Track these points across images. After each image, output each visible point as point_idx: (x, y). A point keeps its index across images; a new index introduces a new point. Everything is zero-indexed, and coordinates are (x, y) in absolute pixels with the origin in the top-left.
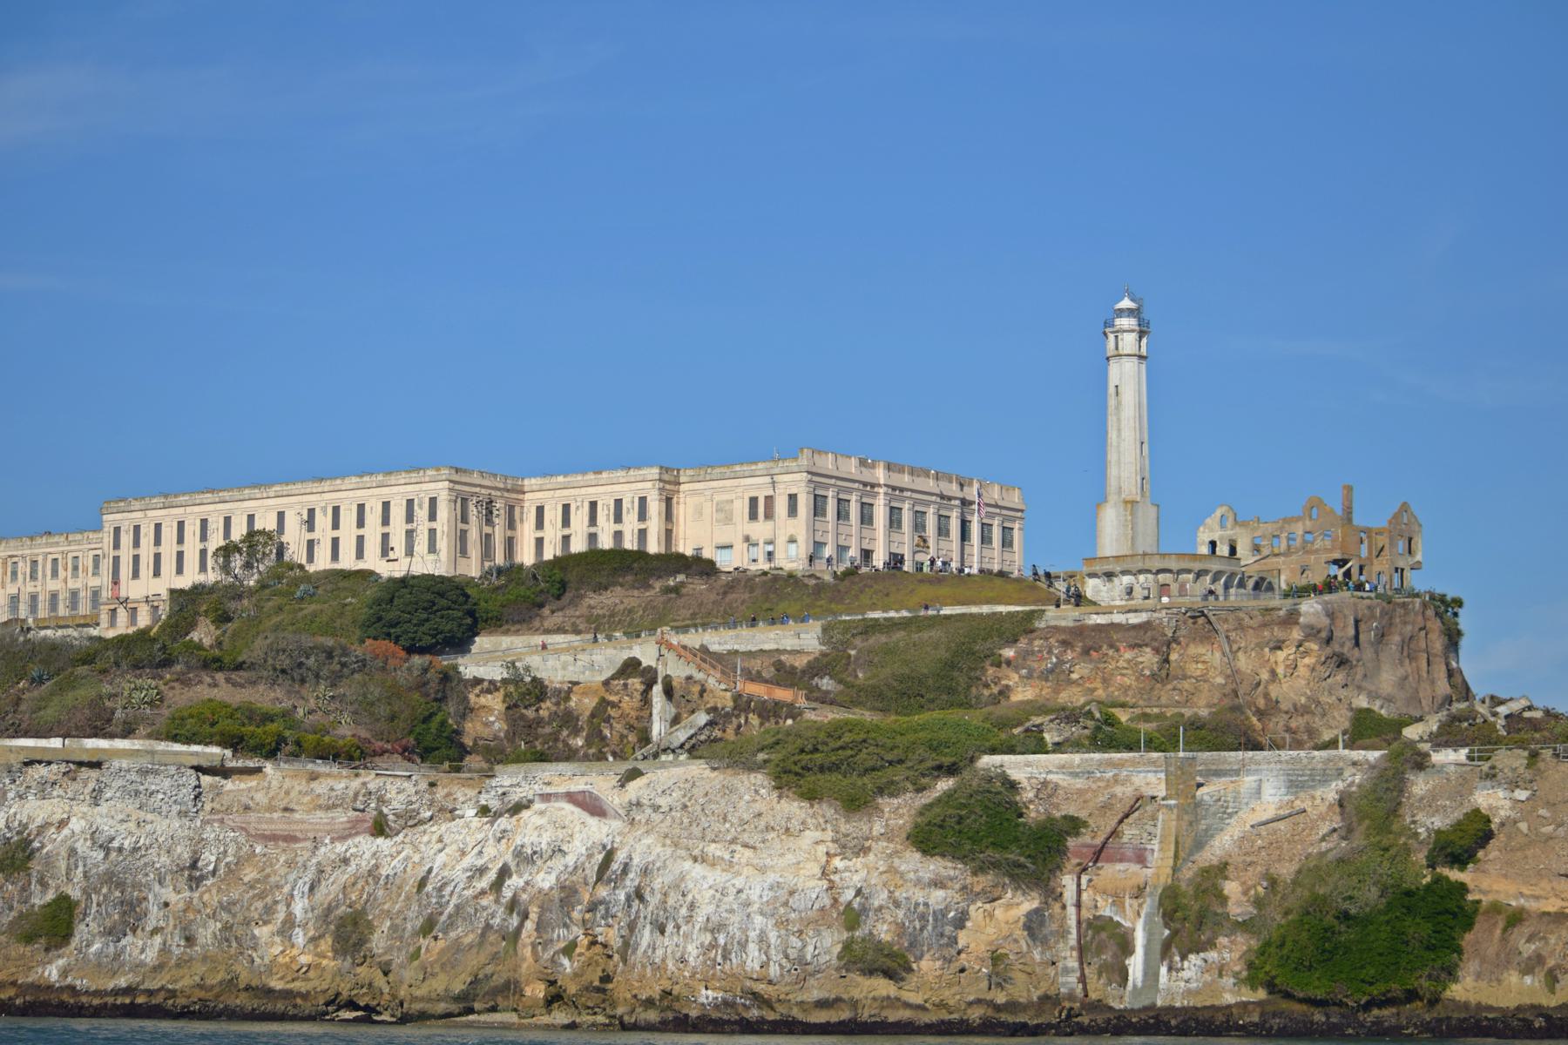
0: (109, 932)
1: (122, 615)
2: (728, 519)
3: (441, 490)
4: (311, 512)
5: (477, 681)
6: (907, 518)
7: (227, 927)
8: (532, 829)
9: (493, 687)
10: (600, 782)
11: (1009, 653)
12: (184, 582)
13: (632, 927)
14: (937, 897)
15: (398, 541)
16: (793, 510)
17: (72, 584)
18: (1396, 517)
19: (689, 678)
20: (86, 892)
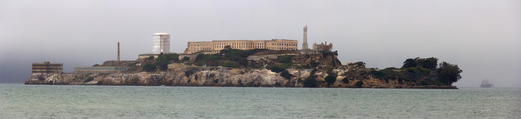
0: (221, 82)
1: (214, 52)
2: (270, 45)
4: (233, 43)
5: (249, 60)
6: (286, 45)
7: (231, 81)
8: (254, 74)
9: (250, 61)
10: (259, 71)
11: (293, 58)
12: (221, 49)
14: (282, 79)
15: (241, 46)
16: (276, 45)
17: (207, 47)
20: (219, 78)
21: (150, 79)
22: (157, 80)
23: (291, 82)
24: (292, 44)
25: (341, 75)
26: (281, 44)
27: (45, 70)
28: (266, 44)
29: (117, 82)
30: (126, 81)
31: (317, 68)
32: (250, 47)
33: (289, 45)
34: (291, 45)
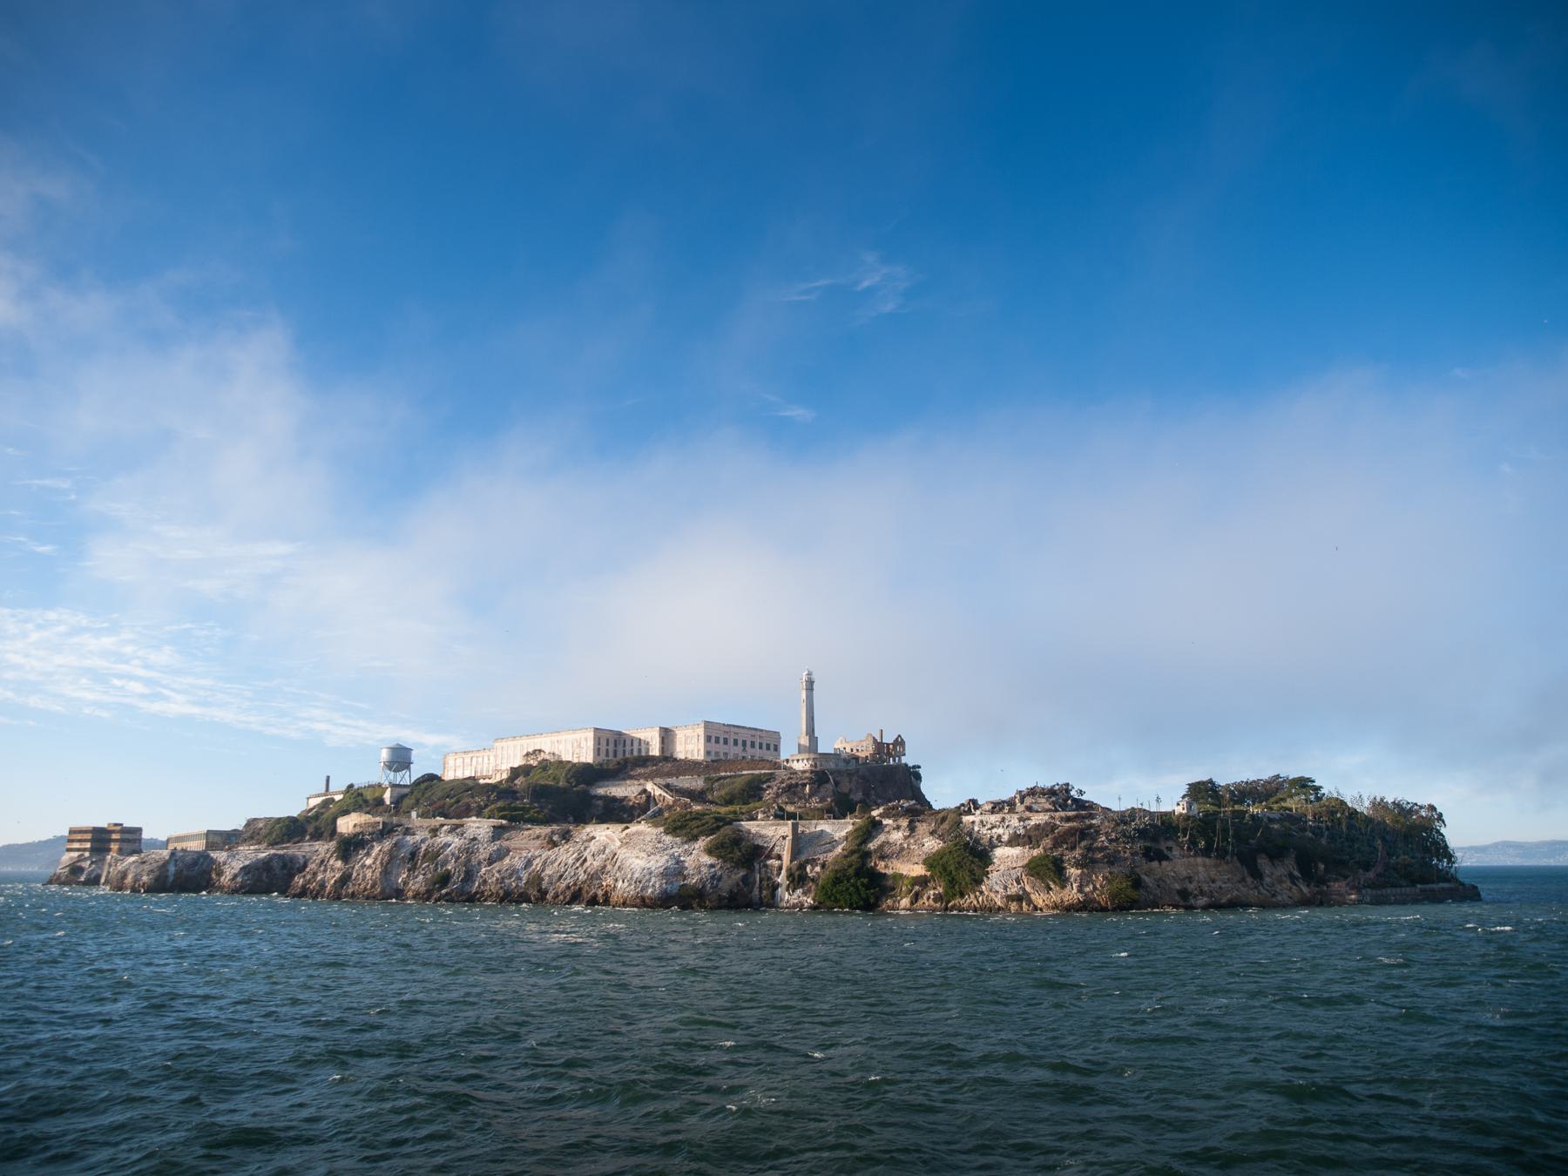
3: (591, 735)
6: (740, 742)
11: (764, 786)
13: (616, 880)
18: (897, 739)
19: (660, 795)
21: (257, 869)
22: (285, 871)
23: (755, 882)
24: (761, 745)
25: (1014, 841)
26: (722, 741)
27: (88, 845)
28: (666, 741)
29: (145, 878)
30: (178, 873)
31: (875, 813)
32: (611, 754)
33: (748, 744)
34: (757, 745)
